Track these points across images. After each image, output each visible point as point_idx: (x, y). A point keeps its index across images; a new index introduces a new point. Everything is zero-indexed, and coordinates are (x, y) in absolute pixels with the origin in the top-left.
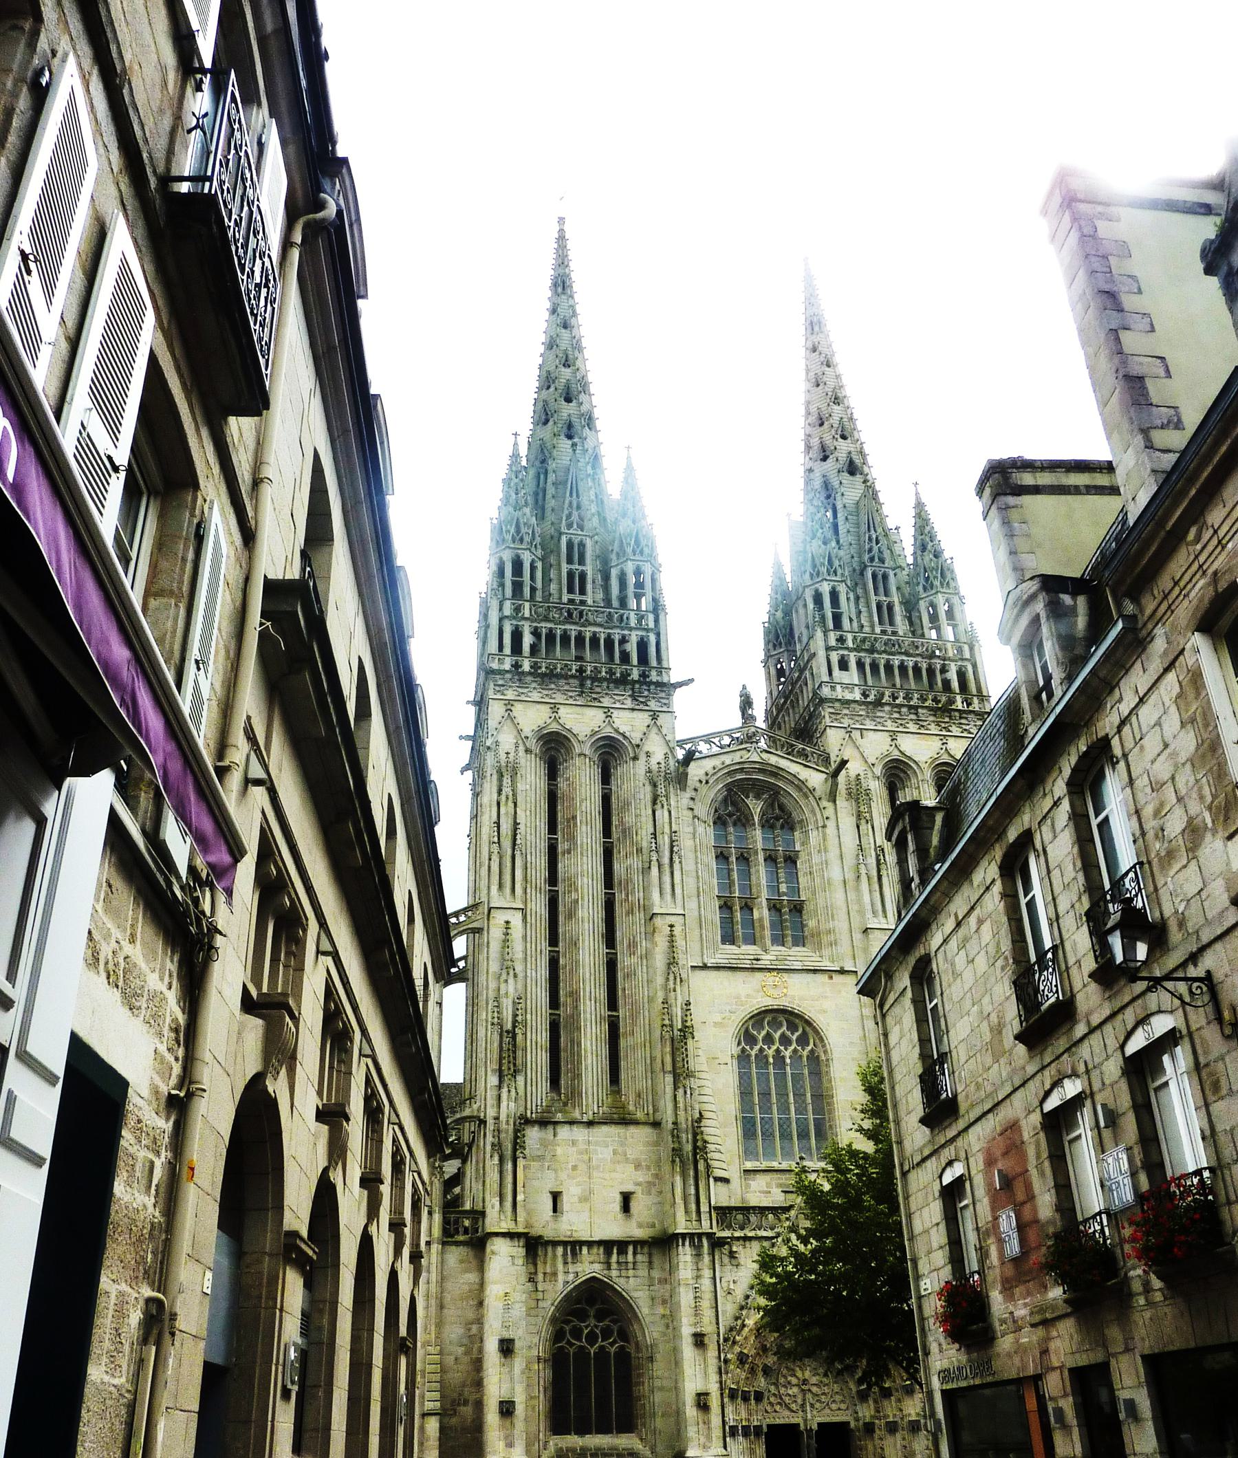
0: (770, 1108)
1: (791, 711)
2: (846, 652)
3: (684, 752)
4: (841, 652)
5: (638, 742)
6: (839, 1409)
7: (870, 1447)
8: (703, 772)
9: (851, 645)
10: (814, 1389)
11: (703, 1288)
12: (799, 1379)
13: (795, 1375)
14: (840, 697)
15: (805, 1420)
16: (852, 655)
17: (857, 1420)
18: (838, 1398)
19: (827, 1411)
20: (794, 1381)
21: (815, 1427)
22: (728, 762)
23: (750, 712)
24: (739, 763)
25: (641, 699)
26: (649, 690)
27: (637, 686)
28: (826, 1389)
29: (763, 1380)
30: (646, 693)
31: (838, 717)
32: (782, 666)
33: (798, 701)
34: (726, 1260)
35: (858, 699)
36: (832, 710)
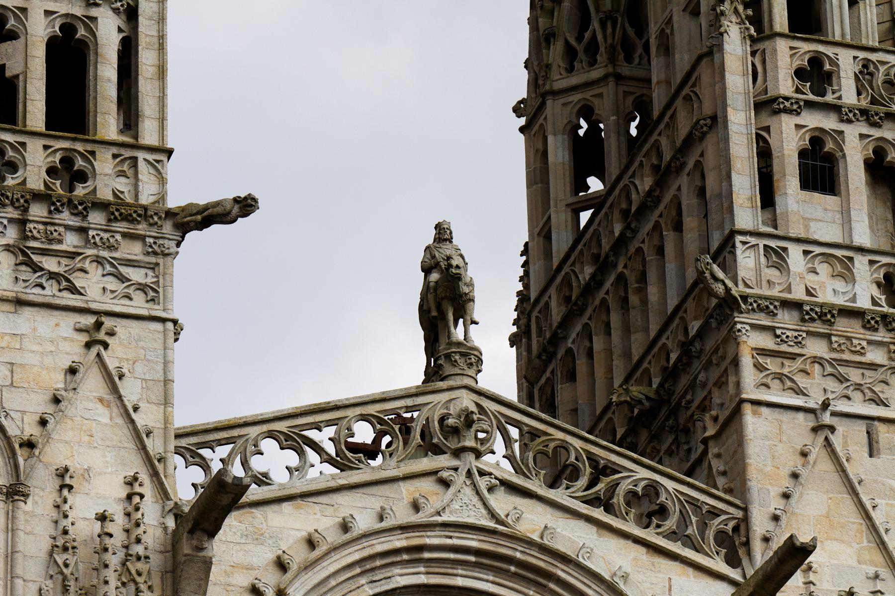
1: (615, 319)
2: (829, 122)
3: (197, 475)
4: (813, 120)
5: (31, 430)
8: (265, 555)
9: (849, 95)
14: (799, 294)
16: (852, 132)
22: (364, 522)
23: (459, 333)
24: (404, 528)
25: (50, 264)
26: (82, 231)
27: (37, 211)
30: (71, 241)
31: (789, 367)
32: (593, 129)
33: (643, 278)
35: (863, 303)
36: (766, 341)
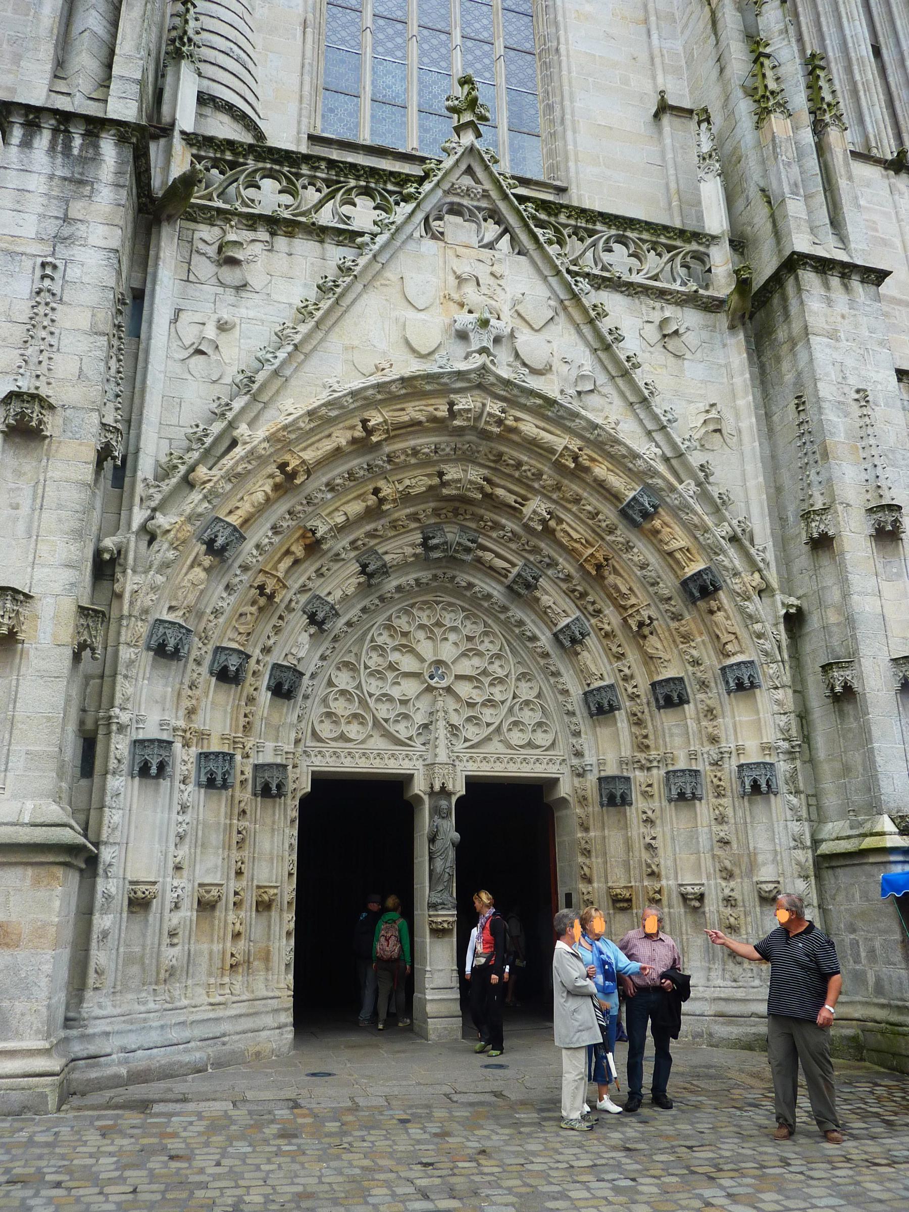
0: (403, 48)
6: (530, 745)
7: (615, 841)
10: (464, 690)
11: (74, 273)
12: (422, 660)
13: (412, 651)
15: (430, 766)
17: (581, 774)
18: (529, 717)
19: (495, 747)
20: (408, 663)
21: (460, 789)
28: (497, 693)
29: (304, 638)
34: (204, 268)
